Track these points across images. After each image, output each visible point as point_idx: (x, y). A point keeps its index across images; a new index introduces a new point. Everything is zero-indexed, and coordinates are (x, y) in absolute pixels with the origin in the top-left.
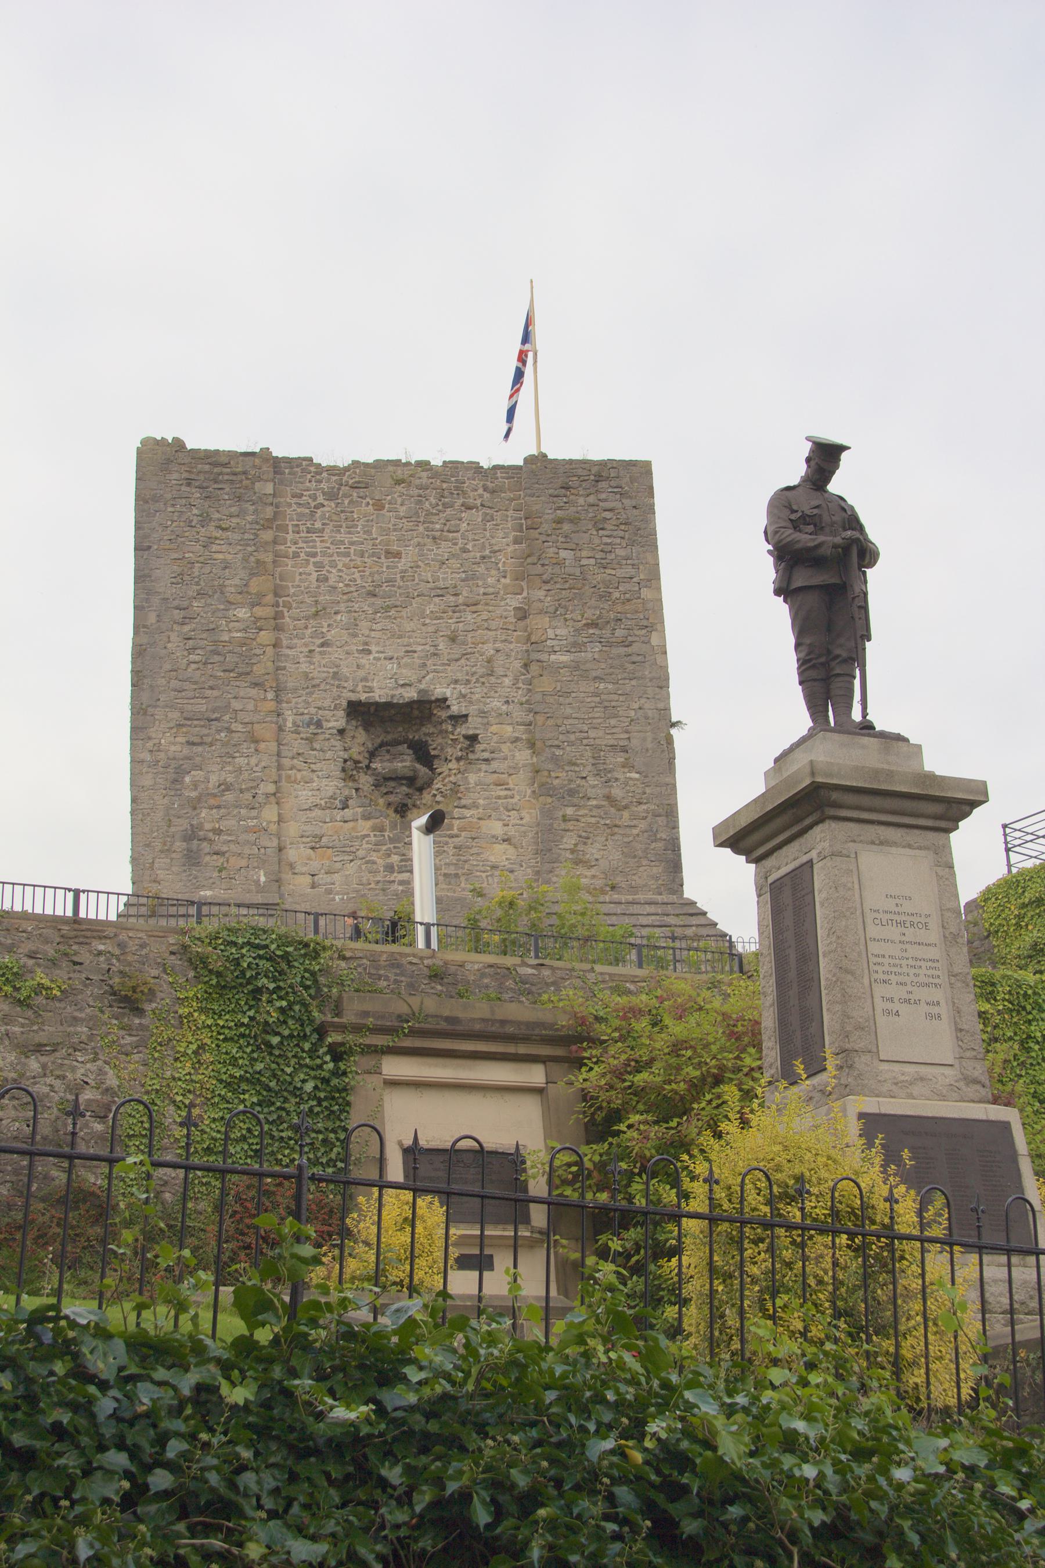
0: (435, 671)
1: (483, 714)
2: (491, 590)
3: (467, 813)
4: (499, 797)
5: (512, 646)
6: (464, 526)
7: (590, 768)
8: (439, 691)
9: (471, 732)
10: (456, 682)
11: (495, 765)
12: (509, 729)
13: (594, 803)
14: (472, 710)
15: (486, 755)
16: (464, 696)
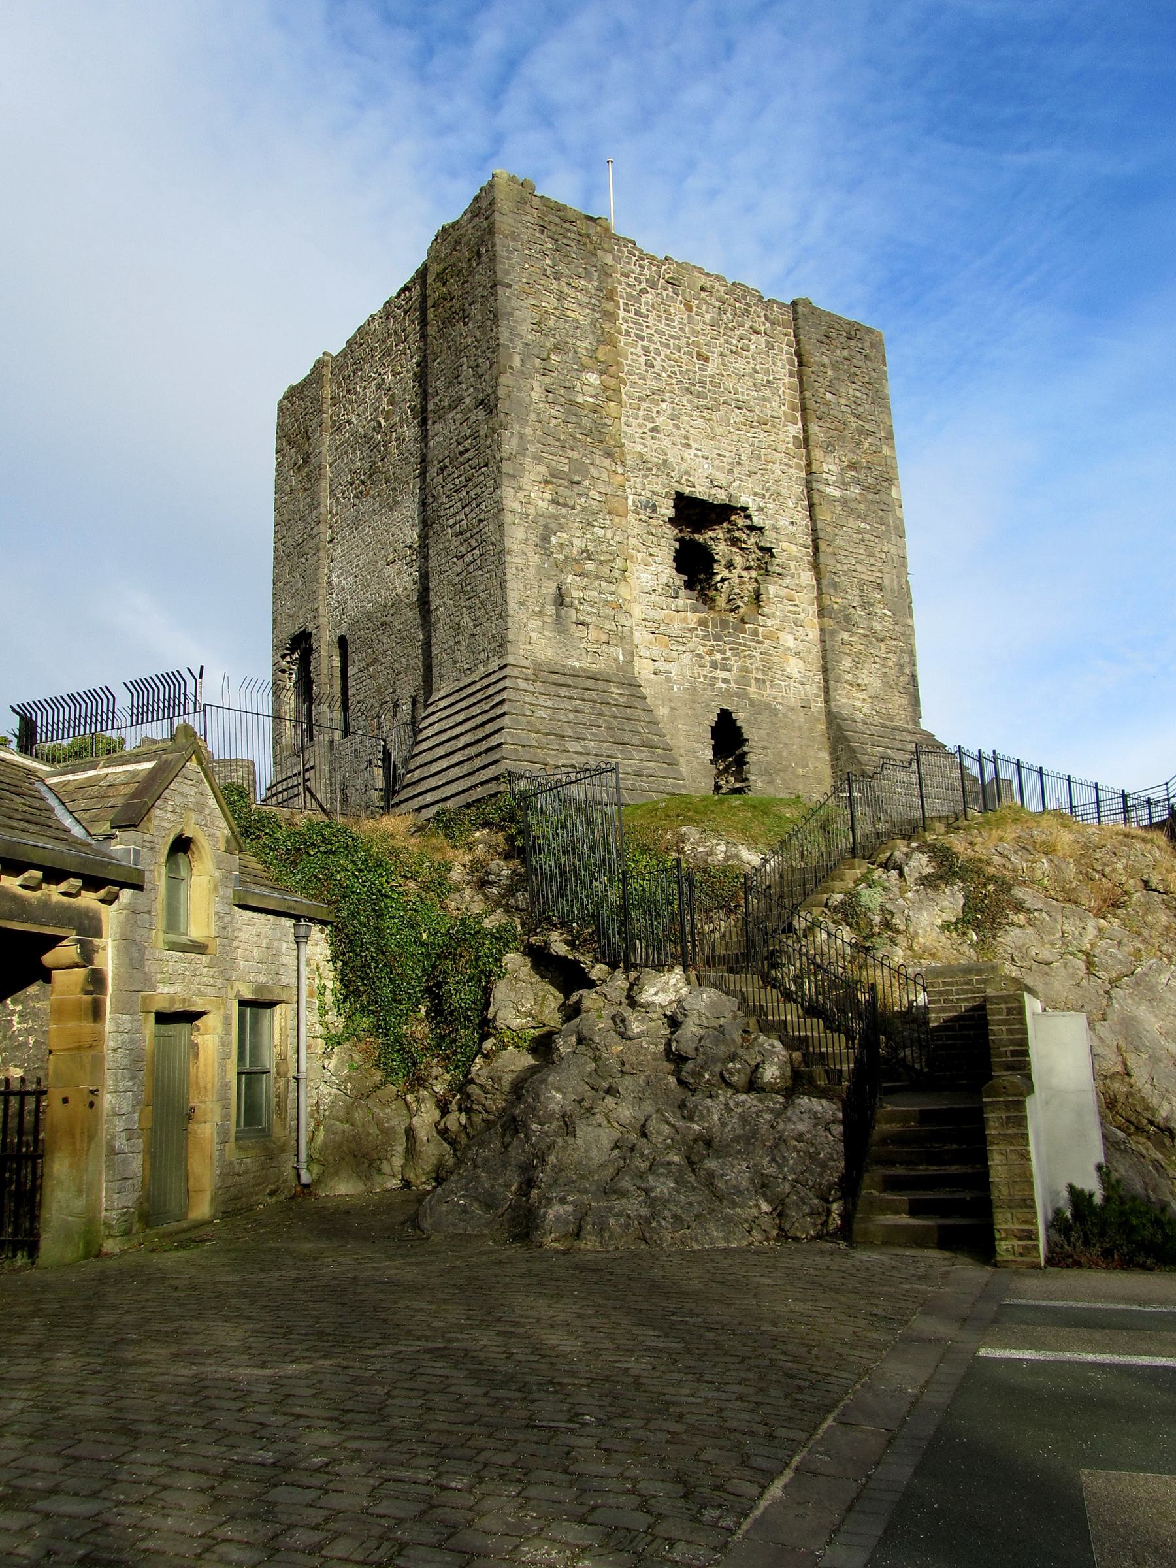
0: (740, 479)
1: (775, 529)
2: (775, 414)
3: (769, 622)
4: (790, 612)
5: (793, 471)
6: (753, 347)
7: (857, 598)
8: (745, 500)
9: (768, 545)
10: (755, 494)
11: (787, 581)
12: (794, 548)
13: (862, 632)
14: (768, 524)
15: (778, 569)
16: (762, 509)
